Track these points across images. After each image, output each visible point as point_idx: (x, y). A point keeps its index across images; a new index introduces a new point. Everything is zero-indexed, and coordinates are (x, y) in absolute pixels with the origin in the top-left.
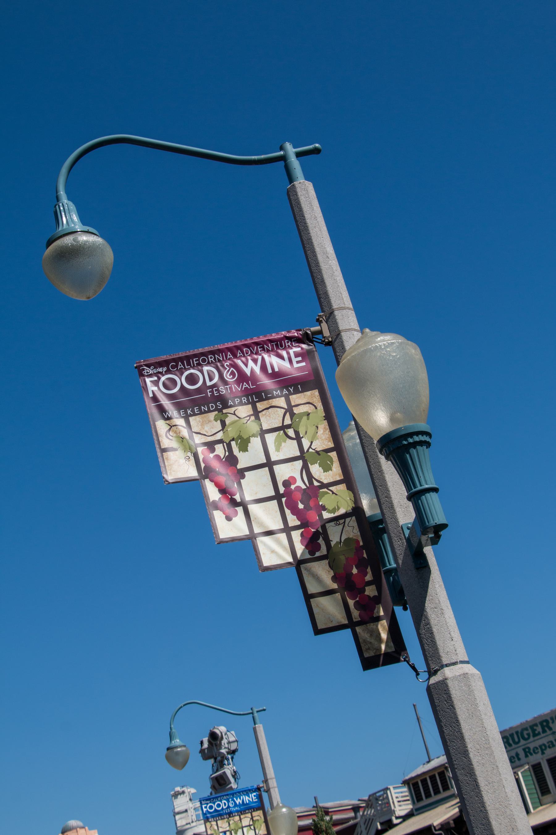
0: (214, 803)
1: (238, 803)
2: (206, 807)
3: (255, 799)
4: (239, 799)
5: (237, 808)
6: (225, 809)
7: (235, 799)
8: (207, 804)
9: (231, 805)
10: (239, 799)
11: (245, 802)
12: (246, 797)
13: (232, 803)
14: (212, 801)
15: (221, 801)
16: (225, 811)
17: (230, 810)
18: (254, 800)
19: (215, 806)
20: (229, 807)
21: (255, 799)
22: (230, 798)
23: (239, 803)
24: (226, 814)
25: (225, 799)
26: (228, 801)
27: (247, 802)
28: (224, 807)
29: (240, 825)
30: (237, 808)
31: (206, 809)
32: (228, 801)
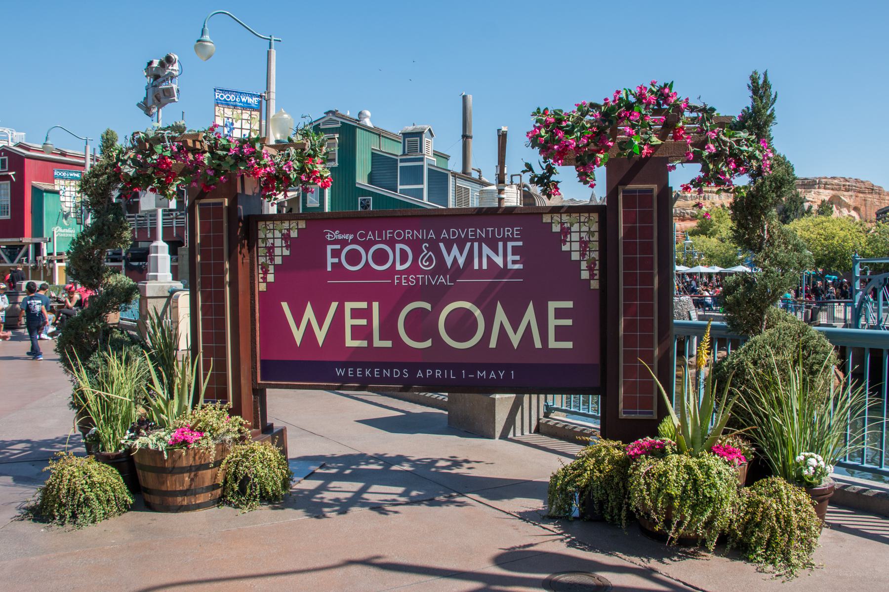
0: (367, 246)
1: (449, 261)
2: (336, 254)
3: (514, 262)
4: (455, 250)
5: (442, 279)
6: (401, 273)
7: (442, 245)
8: (344, 243)
9: (423, 265)
10: (455, 250)
11: (476, 267)
12: (484, 245)
13: (430, 260)
14: (361, 236)
15: (392, 243)
16: (400, 279)
17: (417, 279)
18: (510, 266)
19: (225, 97)
20: (414, 269)
21: (514, 262)
22: (427, 241)
23: (455, 260)
24: (232, 105)
25: (403, 242)
26: (417, 252)
27: (485, 267)
28: (399, 267)
29: (241, 117)
30: (442, 279)
31: (336, 260)
32: (417, 252)
